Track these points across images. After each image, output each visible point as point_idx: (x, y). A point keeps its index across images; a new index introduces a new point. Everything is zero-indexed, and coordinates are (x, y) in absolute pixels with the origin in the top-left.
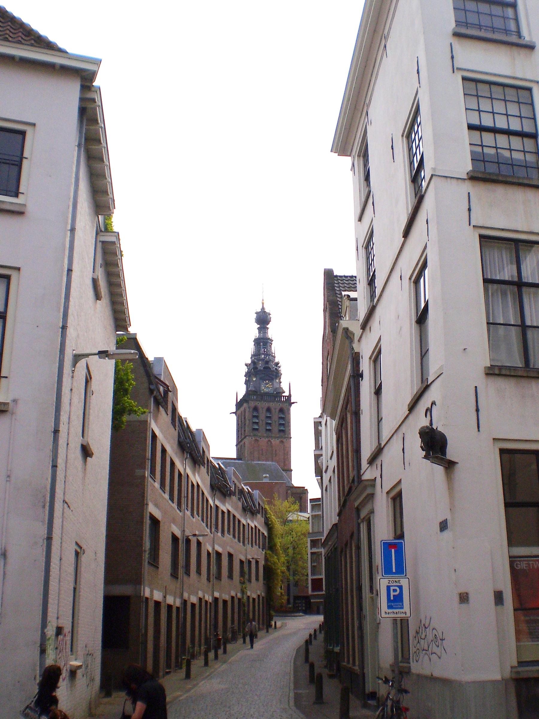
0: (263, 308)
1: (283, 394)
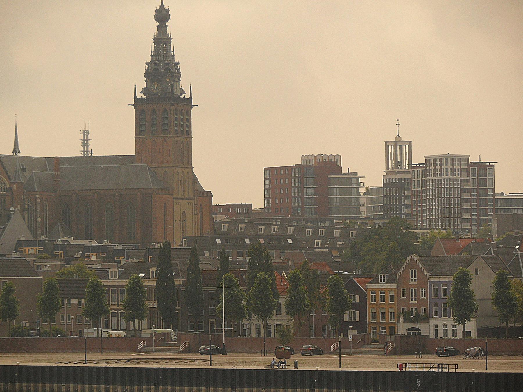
0: (162, 6)
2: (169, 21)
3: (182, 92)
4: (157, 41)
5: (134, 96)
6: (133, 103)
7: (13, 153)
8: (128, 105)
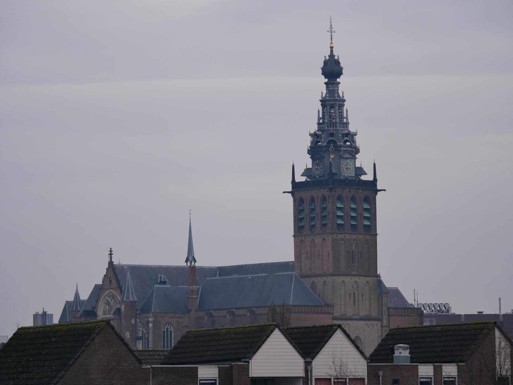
0: (332, 56)
1: (363, 178)
2: (342, 77)
3: (360, 171)
4: (324, 102)
5: (291, 180)
6: (290, 190)
7: (187, 261)
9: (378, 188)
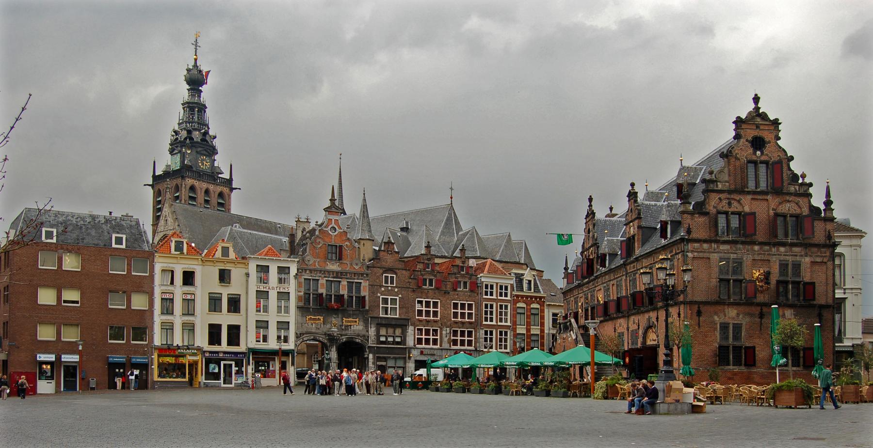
1: (220, 176)
8: (145, 185)
9: (233, 187)
